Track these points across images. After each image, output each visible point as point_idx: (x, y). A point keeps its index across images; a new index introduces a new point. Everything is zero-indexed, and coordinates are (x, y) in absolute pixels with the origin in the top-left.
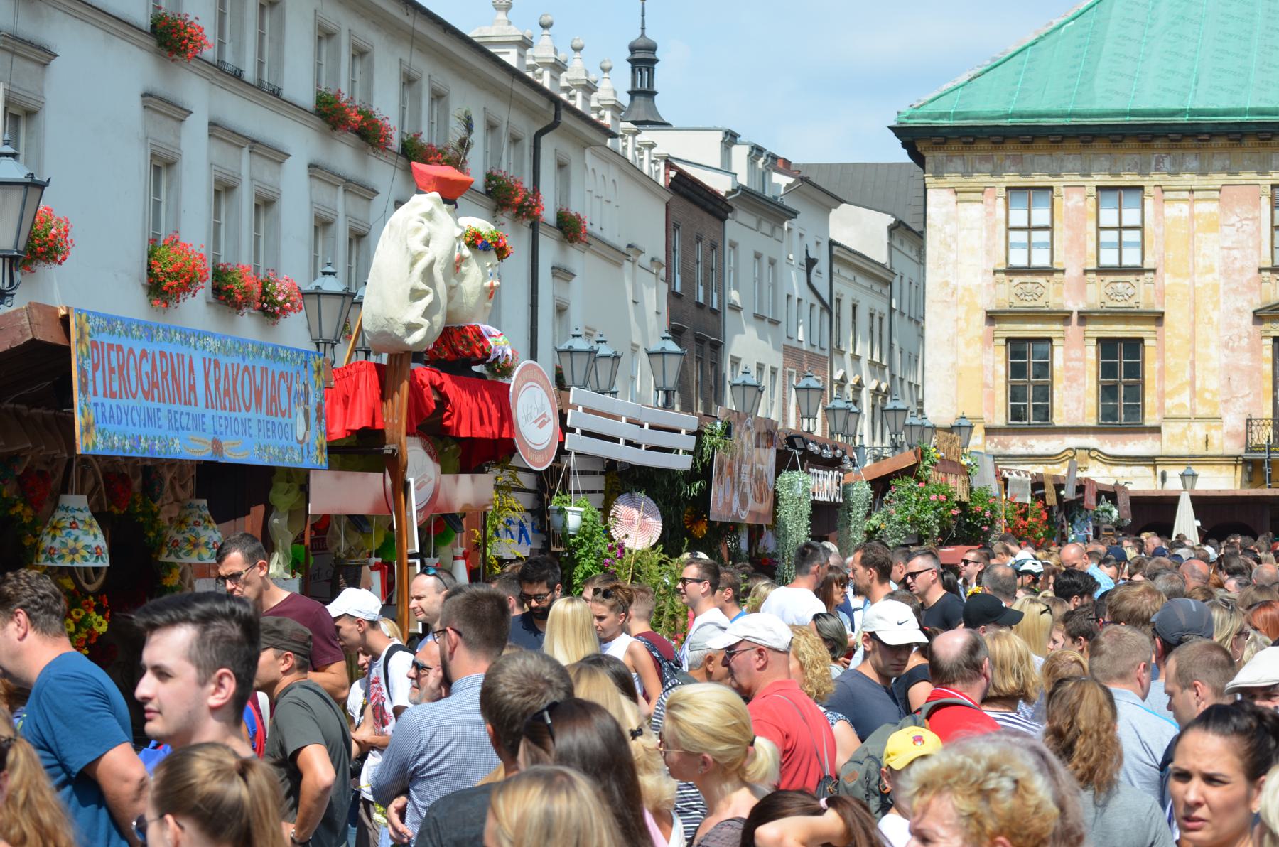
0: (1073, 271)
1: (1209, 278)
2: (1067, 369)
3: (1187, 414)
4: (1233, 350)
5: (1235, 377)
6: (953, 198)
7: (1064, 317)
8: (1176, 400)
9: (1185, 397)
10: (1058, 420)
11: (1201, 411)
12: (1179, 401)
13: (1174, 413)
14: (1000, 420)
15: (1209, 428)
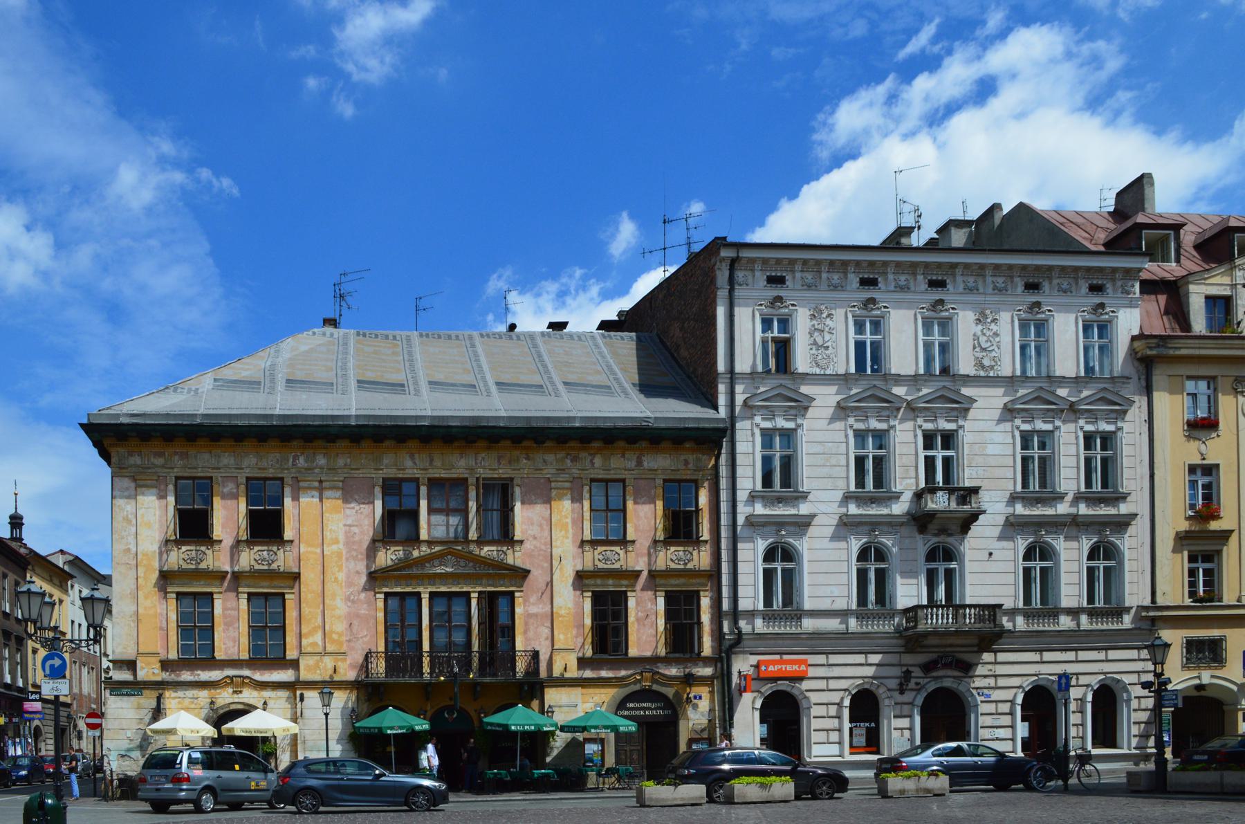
0: (228, 542)
1: (335, 547)
2: (225, 616)
3: (320, 650)
4: (353, 602)
5: (356, 622)
6: (133, 485)
7: (221, 576)
8: (311, 640)
9: (318, 638)
10: (219, 655)
11: (330, 648)
12: (313, 640)
13: (309, 650)
14: (173, 655)
15: (336, 661)
